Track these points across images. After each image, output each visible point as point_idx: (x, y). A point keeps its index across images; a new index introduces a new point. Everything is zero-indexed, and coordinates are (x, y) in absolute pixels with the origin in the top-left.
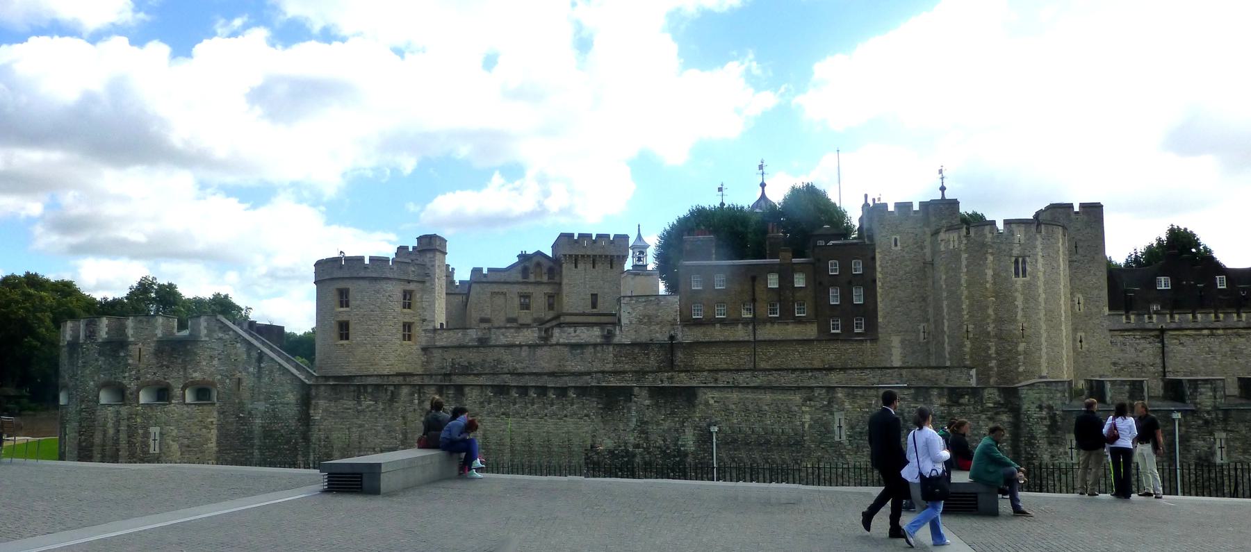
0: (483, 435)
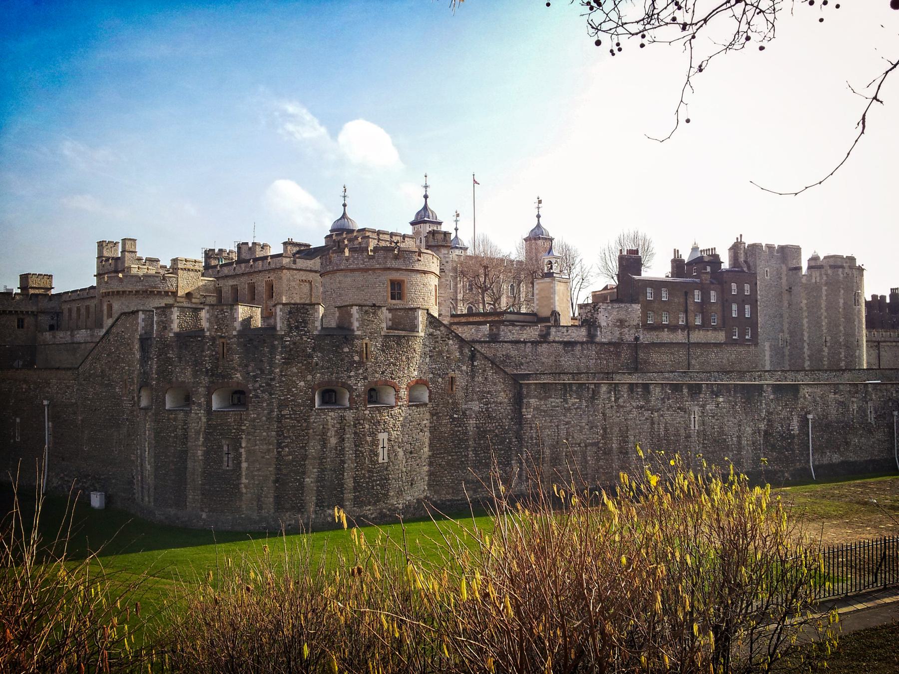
0: (665, 428)
